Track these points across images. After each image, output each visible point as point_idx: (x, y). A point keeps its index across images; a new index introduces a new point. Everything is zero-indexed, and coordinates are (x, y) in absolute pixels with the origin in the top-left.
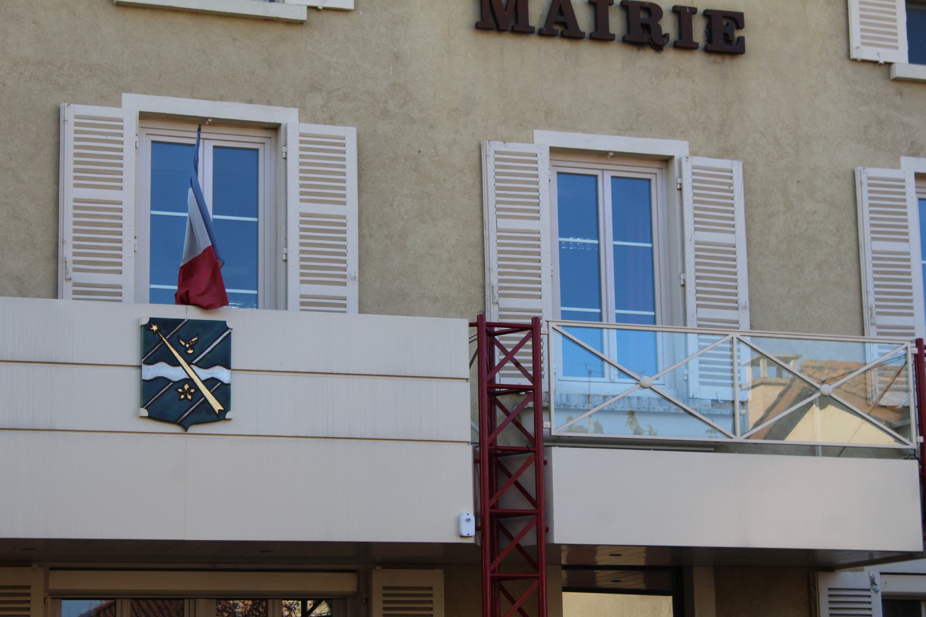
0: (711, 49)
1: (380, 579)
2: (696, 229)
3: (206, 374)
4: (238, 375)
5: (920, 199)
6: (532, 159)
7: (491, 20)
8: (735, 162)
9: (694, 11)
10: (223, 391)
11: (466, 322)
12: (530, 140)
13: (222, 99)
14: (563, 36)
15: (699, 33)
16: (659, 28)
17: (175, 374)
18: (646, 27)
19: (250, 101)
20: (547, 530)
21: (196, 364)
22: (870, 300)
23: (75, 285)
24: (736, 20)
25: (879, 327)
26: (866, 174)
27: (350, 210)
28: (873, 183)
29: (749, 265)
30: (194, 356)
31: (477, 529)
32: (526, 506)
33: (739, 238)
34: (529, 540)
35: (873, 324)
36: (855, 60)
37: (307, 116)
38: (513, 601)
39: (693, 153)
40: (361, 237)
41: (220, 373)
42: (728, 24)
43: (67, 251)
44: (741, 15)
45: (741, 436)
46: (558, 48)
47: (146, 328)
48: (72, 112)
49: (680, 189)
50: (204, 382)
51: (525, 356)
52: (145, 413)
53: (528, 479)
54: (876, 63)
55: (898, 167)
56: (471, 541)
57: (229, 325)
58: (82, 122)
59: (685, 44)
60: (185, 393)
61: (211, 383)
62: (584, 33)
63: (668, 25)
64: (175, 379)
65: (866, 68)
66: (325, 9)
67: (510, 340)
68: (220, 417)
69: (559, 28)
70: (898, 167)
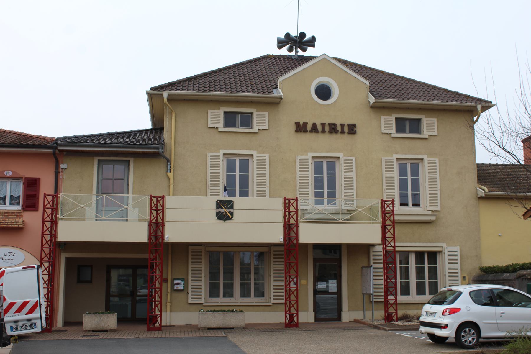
0: (349, 133)
1: (273, 248)
2: (344, 173)
3: (229, 210)
4: (234, 210)
5: (399, 163)
6: (307, 159)
7: (298, 129)
8: (354, 157)
9: (345, 124)
10: (232, 214)
11: (282, 198)
12: (307, 155)
13: (240, 150)
14: (315, 132)
15: (346, 129)
16: (337, 129)
17: (222, 211)
18: (333, 129)
19: (246, 150)
20: (298, 240)
21: (227, 209)
22: (384, 187)
23: (210, 189)
24: (355, 126)
25: (386, 193)
26: (384, 159)
27: (267, 172)
28: (386, 161)
29: (356, 180)
30: (226, 207)
31: (284, 240)
32: (295, 235)
33: (354, 174)
34: (295, 242)
35: (385, 192)
36: (382, 133)
37: (259, 152)
38: (292, 254)
39: (344, 156)
40: (270, 177)
41: (231, 210)
42: (353, 127)
43: (209, 183)
44: (356, 125)
45: (341, 220)
46: (313, 135)
47: (217, 202)
48: (210, 154)
49: (341, 164)
50: (228, 212)
51: (294, 204)
52: (217, 218)
53: (295, 229)
54: (388, 133)
55: (392, 157)
56: (282, 242)
57: (233, 201)
58: (212, 156)
59: (343, 132)
60: (224, 214)
61: (229, 212)
62: (319, 131)
63: (339, 128)
64: (223, 212)
65: (385, 135)
66: (262, 129)
67: (292, 201)
68: (231, 219)
69: (314, 131)
70: (392, 157)
